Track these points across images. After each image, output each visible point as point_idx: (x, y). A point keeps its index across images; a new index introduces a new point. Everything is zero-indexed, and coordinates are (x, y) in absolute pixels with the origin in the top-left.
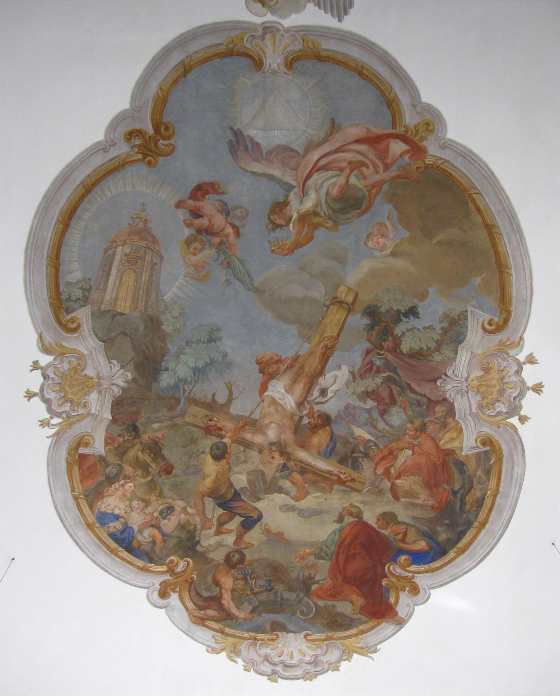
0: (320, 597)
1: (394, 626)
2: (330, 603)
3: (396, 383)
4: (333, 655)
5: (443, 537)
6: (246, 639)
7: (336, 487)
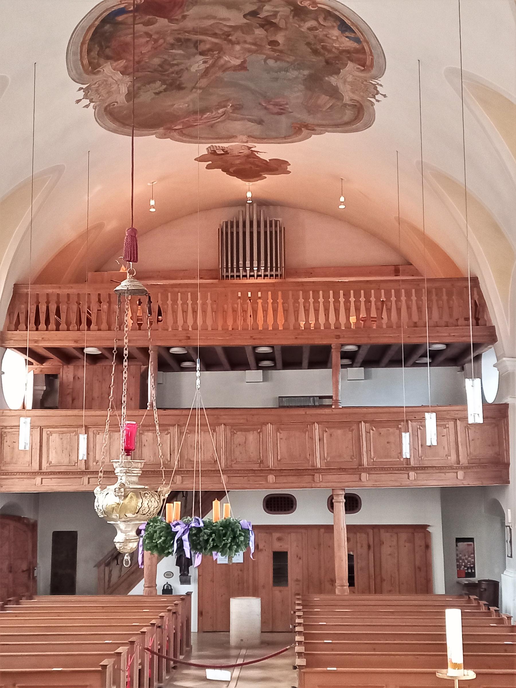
3: (160, 71)
5: (107, 27)
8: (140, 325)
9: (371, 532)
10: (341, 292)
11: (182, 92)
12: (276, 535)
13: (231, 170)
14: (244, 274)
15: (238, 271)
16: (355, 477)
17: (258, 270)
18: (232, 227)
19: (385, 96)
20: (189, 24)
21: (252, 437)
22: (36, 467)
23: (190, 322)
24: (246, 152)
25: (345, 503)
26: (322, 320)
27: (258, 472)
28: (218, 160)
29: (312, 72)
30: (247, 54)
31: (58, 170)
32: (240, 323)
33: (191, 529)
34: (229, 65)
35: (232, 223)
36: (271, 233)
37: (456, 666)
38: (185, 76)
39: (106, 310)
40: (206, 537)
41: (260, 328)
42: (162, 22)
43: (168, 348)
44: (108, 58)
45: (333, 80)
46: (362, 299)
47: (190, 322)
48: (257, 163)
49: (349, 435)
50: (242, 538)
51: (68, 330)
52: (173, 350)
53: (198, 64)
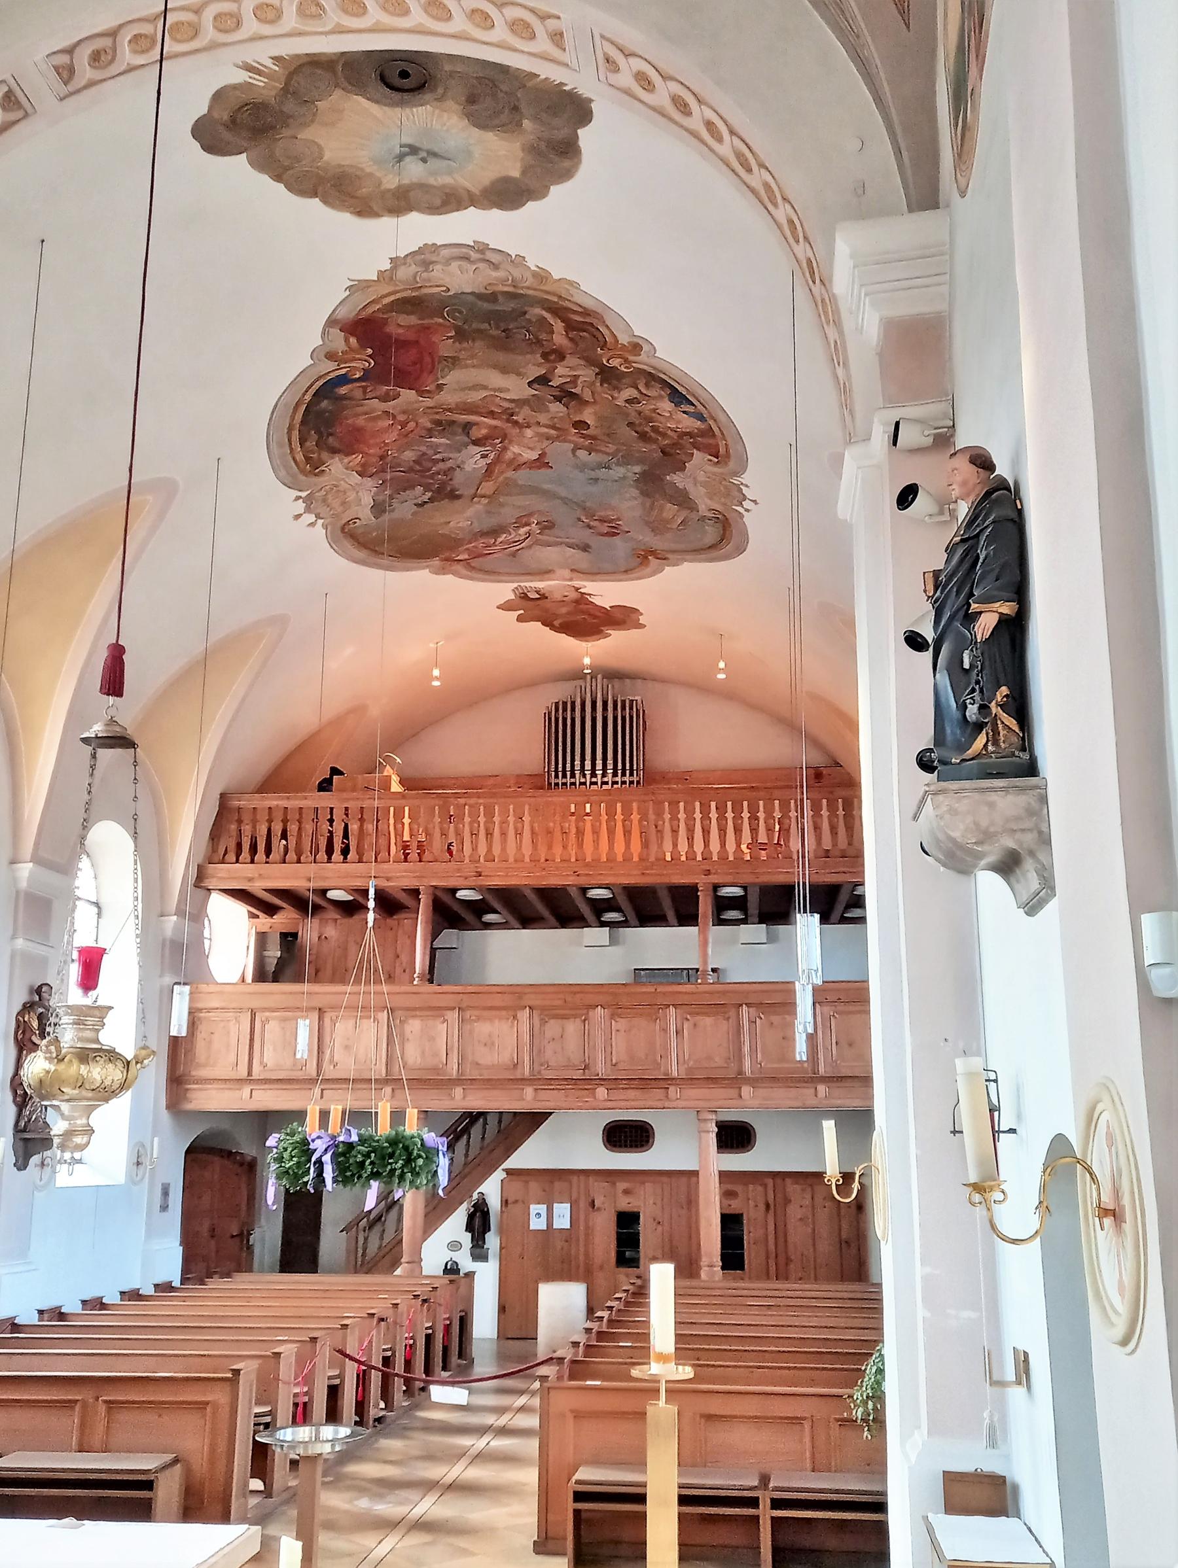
0: (440, 325)
1: (339, 317)
2: (425, 322)
4: (404, 273)
5: (325, 404)
6: (528, 288)
7: (453, 406)
8: (406, 855)
9: (770, 1182)
10: (713, 804)
11: (458, 503)
12: (622, 1185)
13: (557, 623)
14: (583, 780)
15: (573, 776)
16: (733, 1092)
17: (604, 775)
18: (565, 710)
19: (755, 502)
20: (448, 398)
21: (572, 1027)
22: (243, 1072)
23: (482, 849)
24: (573, 595)
25: (718, 1135)
26: (683, 847)
27: (583, 1082)
28: (533, 607)
29: (646, 467)
30: (546, 443)
31: (280, 621)
32: (558, 851)
33: (337, 1146)
34: (522, 460)
35: (565, 704)
36: (624, 718)
37: (662, 1358)
38: (458, 478)
39: (356, 833)
40: (360, 1158)
41: (588, 859)
42: (408, 395)
43: (453, 891)
44: (334, 451)
45: (677, 479)
46: (746, 815)
47: (482, 849)
48: (592, 612)
49: (724, 1026)
50: (420, 1162)
51: (299, 862)
52: (461, 894)
53: (473, 460)
